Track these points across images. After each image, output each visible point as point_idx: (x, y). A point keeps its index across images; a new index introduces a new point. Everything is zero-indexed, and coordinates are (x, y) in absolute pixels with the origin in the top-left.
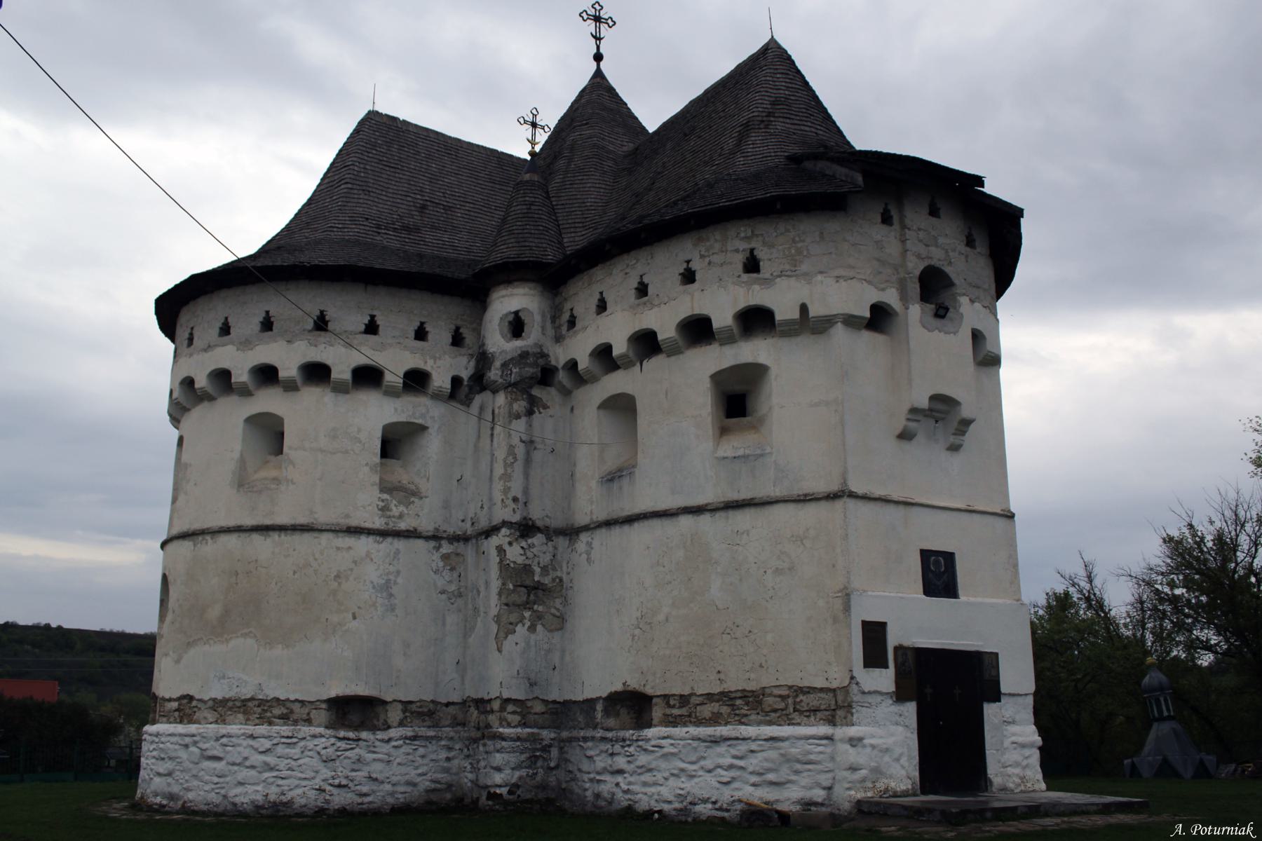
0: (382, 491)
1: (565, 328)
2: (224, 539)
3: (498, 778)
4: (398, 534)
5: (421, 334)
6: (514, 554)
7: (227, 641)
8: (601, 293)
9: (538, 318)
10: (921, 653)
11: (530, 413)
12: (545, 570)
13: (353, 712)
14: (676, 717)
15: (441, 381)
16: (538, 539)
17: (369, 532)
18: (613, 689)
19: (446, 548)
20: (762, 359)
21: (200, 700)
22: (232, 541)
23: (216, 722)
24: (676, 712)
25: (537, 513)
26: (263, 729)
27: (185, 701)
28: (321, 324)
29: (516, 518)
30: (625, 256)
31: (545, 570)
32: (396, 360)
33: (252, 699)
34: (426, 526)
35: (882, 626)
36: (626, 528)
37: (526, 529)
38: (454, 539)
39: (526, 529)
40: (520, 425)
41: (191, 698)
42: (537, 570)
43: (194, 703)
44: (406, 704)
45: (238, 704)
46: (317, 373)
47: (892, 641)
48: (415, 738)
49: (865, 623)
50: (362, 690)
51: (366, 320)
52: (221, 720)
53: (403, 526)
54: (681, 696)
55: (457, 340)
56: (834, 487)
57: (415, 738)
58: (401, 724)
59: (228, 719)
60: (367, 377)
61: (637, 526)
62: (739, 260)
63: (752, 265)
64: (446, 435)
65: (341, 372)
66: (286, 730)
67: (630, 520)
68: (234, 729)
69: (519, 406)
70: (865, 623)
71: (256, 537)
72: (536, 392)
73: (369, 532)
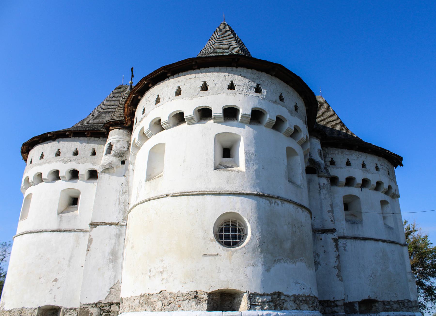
1: (328, 164)
2: (287, 205)
7: (295, 262)
8: (348, 159)
14: (387, 308)
18: (364, 298)
20: (388, 201)
21: (287, 296)
23: (296, 309)
24: (387, 307)
27: (275, 296)
30: (357, 152)
33: (309, 296)
36: (363, 242)
41: (279, 294)
43: (283, 297)
45: (304, 299)
54: (388, 301)
59: (302, 307)
61: (367, 242)
67: (365, 239)
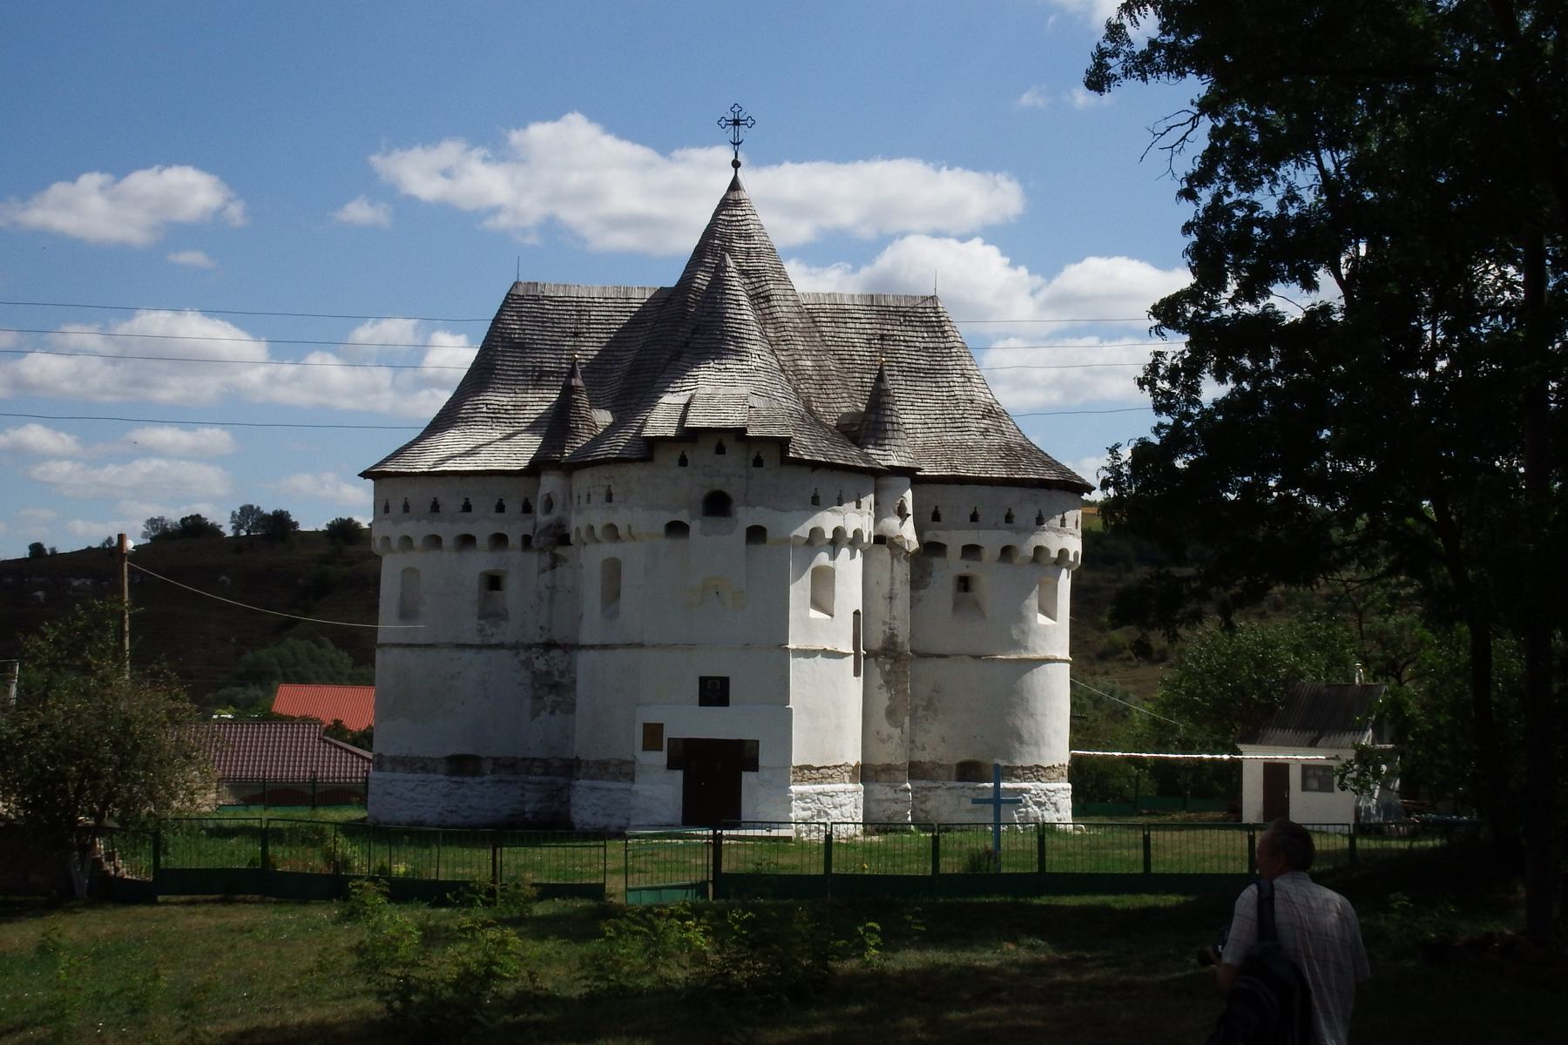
0: (481, 617)
3: (528, 808)
4: (489, 647)
5: (500, 508)
6: (540, 664)
9: (560, 497)
10: (689, 743)
11: (553, 567)
12: (562, 674)
13: (461, 765)
15: (514, 540)
16: (556, 653)
17: (471, 646)
19: (523, 655)
20: (619, 556)
22: (396, 652)
25: (557, 636)
26: (411, 776)
28: (435, 507)
29: (543, 640)
31: (562, 674)
32: (483, 530)
34: (509, 638)
35: (661, 726)
37: (549, 646)
38: (528, 647)
39: (549, 646)
40: (547, 576)
42: (556, 674)
44: (496, 760)
46: (435, 541)
47: (668, 733)
48: (499, 781)
49: (645, 725)
50: (467, 751)
51: (462, 502)
52: (393, 770)
53: (494, 641)
55: (527, 508)
56: (637, 640)
57: (499, 781)
58: (493, 772)
60: (467, 541)
62: (603, 491)
63: (609, 498)
64: (524, 573)
65: (448, 541)
66: (421, 776)
68: (397, 775)
69: (546, 559)
70: (645, 725)
71: (407, 651)
72: (559, 551)
73: (471, 646)
